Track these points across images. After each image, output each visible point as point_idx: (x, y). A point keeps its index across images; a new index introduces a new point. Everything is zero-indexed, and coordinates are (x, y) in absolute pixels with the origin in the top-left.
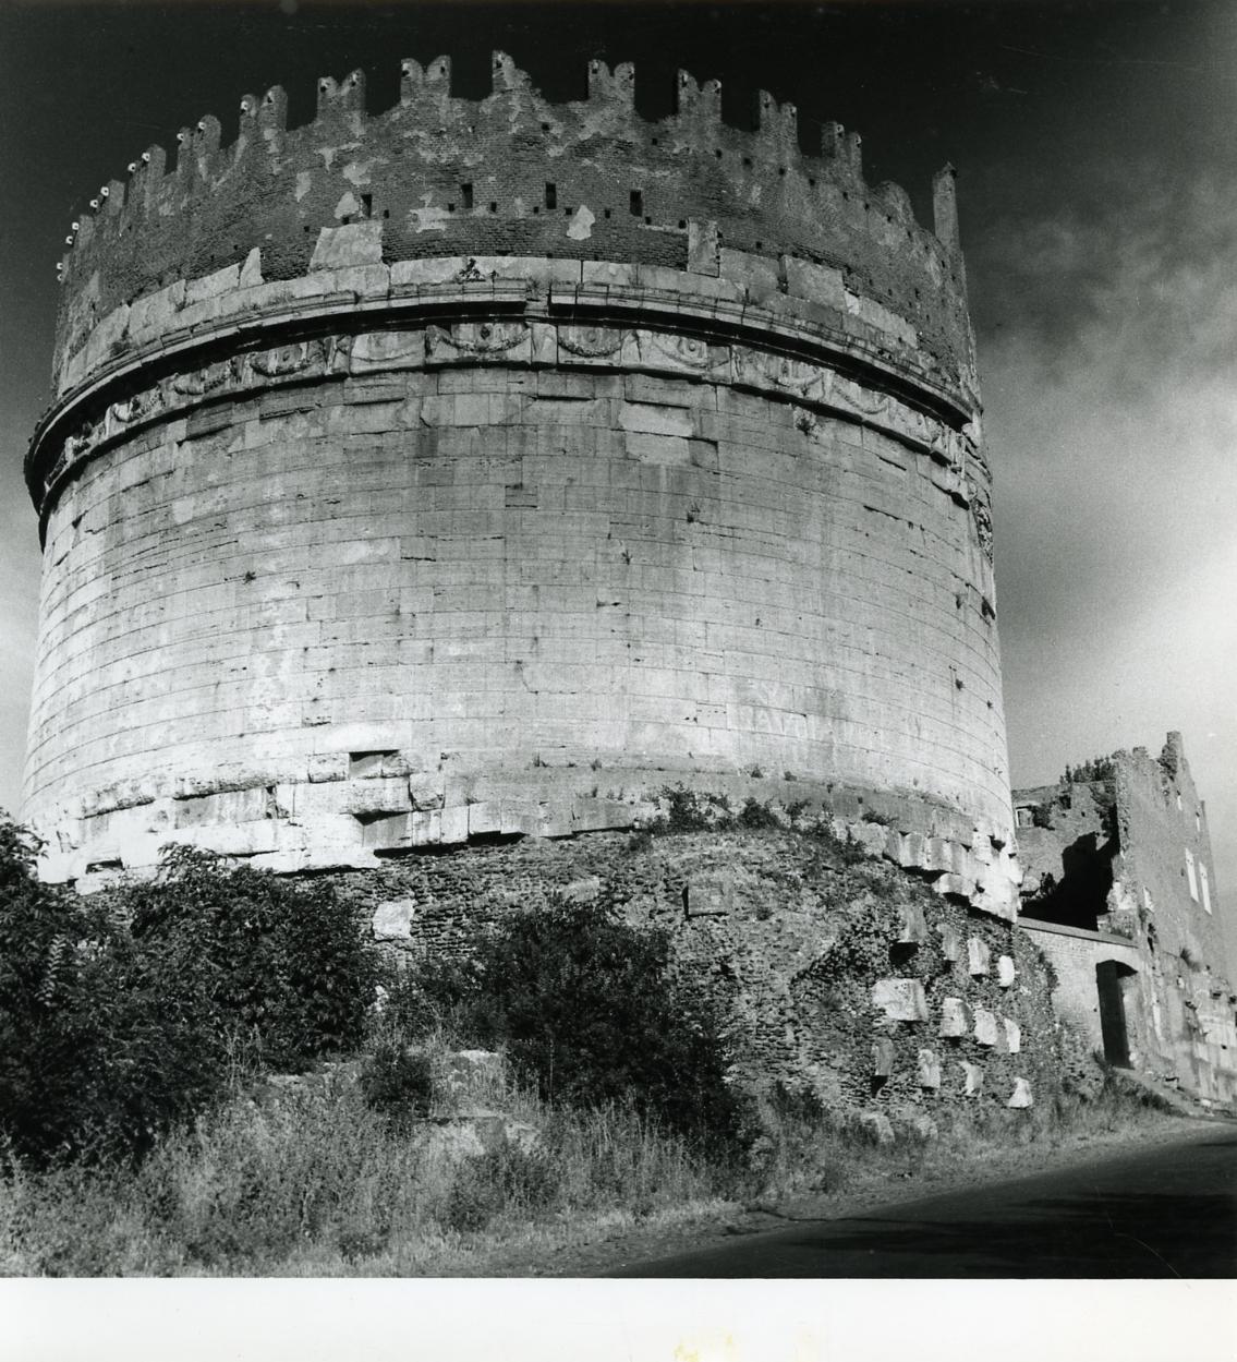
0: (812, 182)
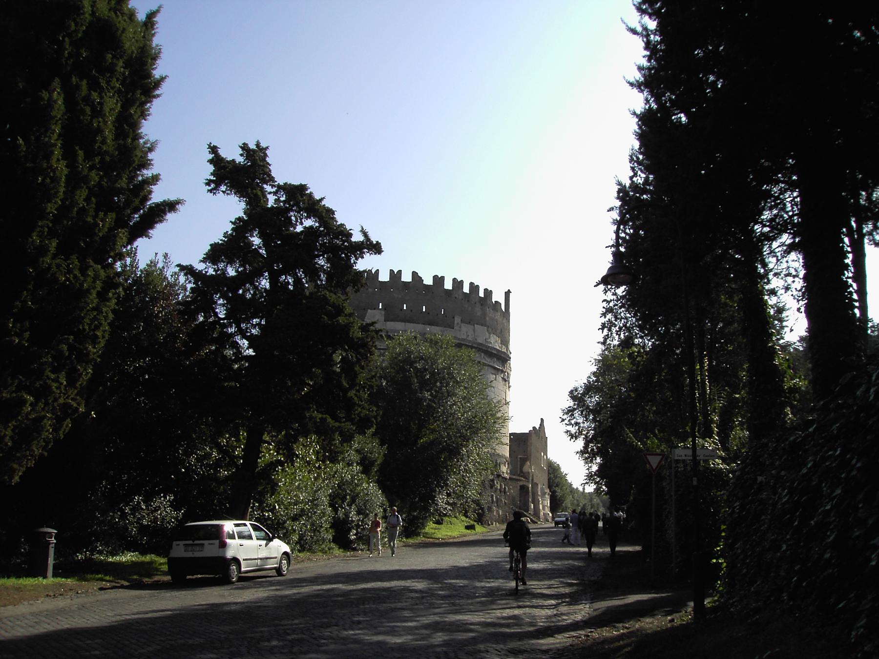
0: (482, 305)
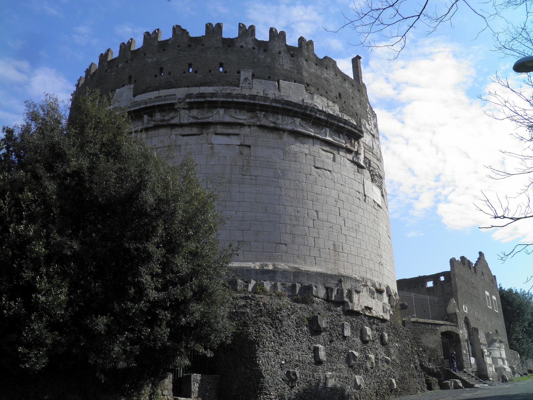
0: (292, 56)
